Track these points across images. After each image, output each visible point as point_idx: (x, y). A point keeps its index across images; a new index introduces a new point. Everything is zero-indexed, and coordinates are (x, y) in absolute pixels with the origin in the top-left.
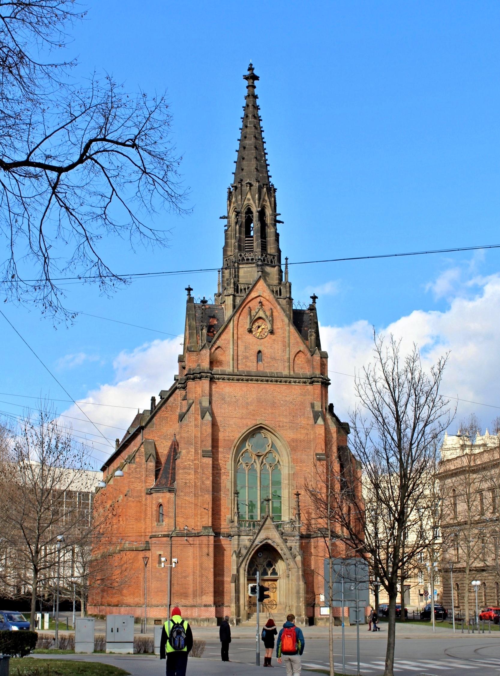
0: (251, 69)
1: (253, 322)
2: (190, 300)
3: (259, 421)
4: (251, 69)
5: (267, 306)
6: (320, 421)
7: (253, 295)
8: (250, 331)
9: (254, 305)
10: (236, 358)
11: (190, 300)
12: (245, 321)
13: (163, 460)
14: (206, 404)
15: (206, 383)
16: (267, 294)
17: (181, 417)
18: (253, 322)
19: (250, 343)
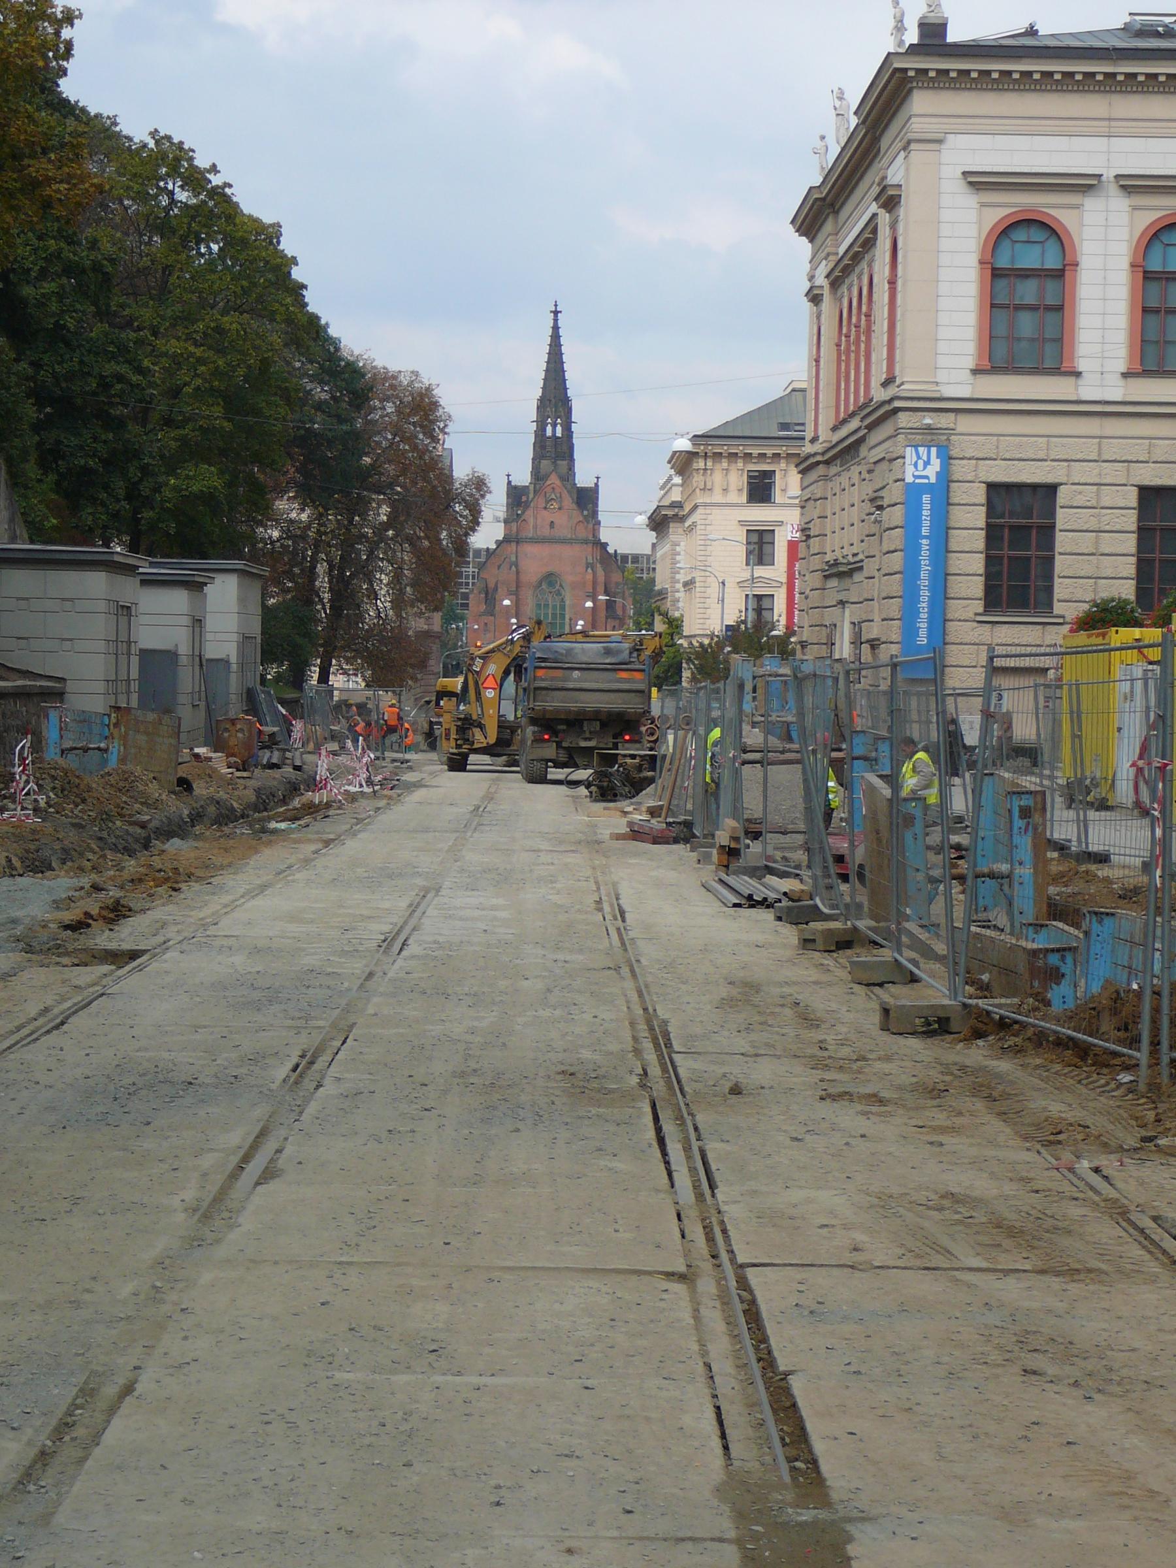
0: (556, 305)
1: (547, 502)
2: (509, 483)
3: (550, 569)
4: (556, 305)
5: (557, 490)
6: (589, 570)
7: (549, 482)
8: (545, 508)
9: (548, 490)
10: (535, 527)
11: (509, 483)
12: (541, 502)
13: (490, 591)
14: (514, 559)
15: (514, 545)
16: (558, 482)
17: (499, 567)
18: (547, 502)
19: (546, 516)
